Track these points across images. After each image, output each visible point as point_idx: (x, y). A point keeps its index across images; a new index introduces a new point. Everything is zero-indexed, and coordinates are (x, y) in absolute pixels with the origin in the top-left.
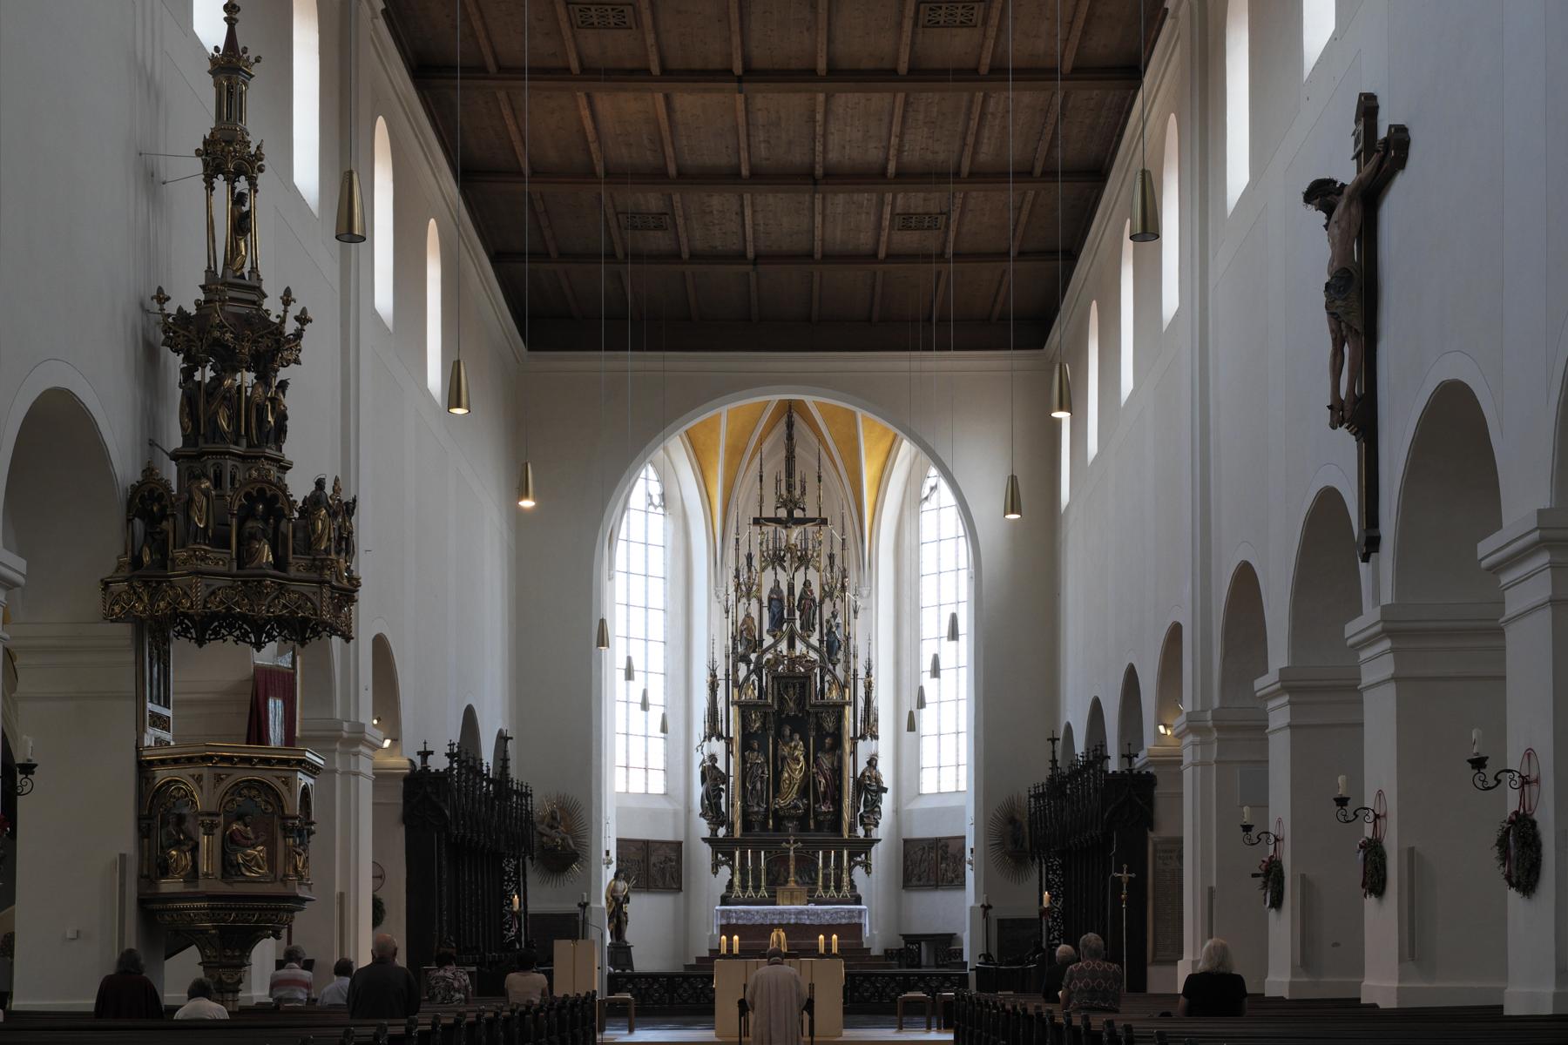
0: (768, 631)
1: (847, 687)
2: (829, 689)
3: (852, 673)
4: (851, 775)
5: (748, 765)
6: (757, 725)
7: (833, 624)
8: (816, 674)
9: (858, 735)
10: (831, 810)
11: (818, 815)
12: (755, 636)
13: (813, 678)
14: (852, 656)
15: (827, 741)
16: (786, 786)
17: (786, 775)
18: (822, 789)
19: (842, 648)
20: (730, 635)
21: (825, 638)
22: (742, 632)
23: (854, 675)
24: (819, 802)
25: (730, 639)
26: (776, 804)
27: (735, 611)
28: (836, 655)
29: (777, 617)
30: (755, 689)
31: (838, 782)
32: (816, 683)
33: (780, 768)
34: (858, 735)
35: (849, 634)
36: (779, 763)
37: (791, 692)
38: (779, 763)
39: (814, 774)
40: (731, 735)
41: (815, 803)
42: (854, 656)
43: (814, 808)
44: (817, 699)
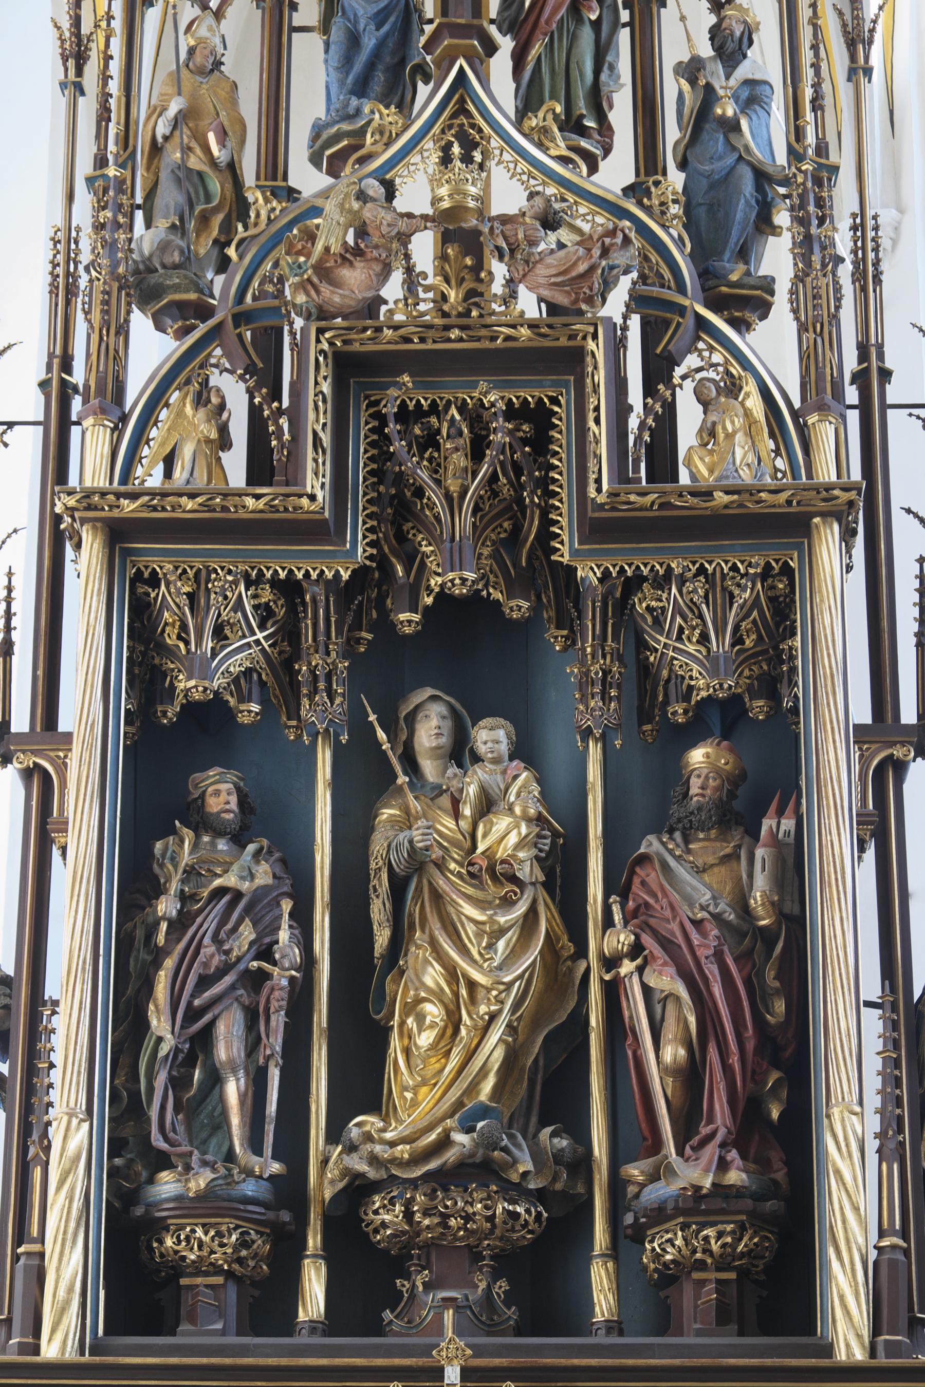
0: (317, 130)
1: (822, 408)
2: (708, 433)
3: (851, 363)
4: (872, 988)
5: (167, 906)
6: (237, 664)
7: (726, 85)
8: (618, 345)
9: (909, 715)
10: (735, 1177)
11: (638, 1236)
12: (232, 169)
13: (597, 349)
14: (845, 271)
15: (697, 756)
16: (425, 1039)
17: (433, 976)
18: (673, 1052)
19: (782, 218)
20: (85, 166)
21: (676, 179)
22: (155, 150)
23: (861, 378)
24: (656, 1145)
25: (84, 200)
26: (351, 1148)
27: (117, 47)
28: (744, 254)
29: (369, 42)
30: (224, 442)
31: (780, 1006)
32: (619, 384)
33: (382, 938)
34: (909, 715)
35: (822, 149)
36: (379, 910)
37: (459, 460)
38: (379, 910)
39: (610, 962)
40: (65, 724)
41: (616, 1161)
42: (859, 275)
43: (617, 1185)
44: (621, 475)
